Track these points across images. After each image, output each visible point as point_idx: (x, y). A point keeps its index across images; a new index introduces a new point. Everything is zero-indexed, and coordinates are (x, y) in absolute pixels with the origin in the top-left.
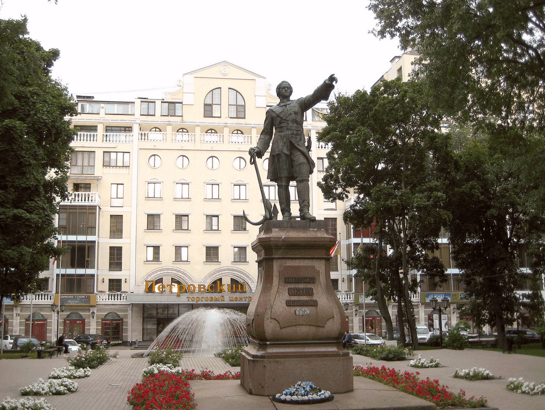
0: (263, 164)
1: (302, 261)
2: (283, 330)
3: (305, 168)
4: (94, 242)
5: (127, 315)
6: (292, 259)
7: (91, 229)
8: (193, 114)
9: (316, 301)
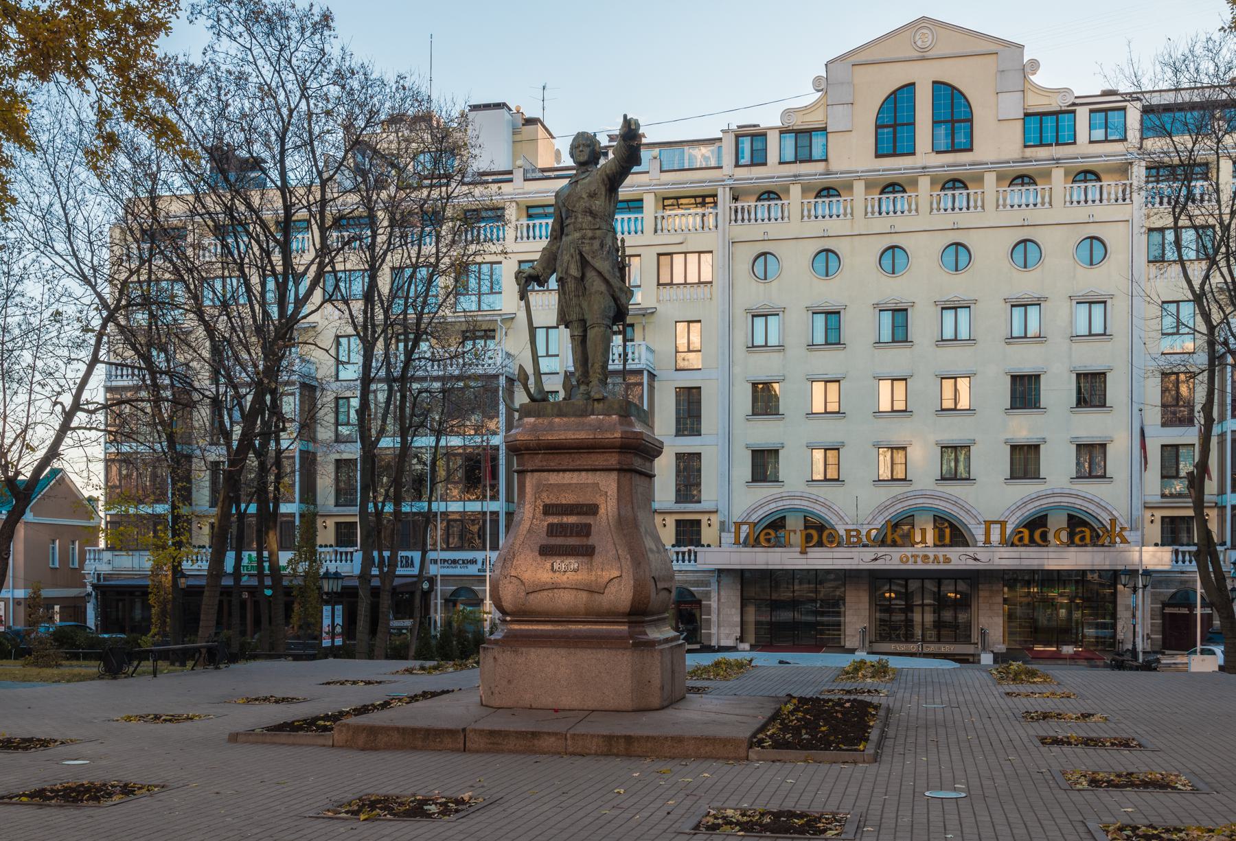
5: (709, 592)
8: (853, 152)
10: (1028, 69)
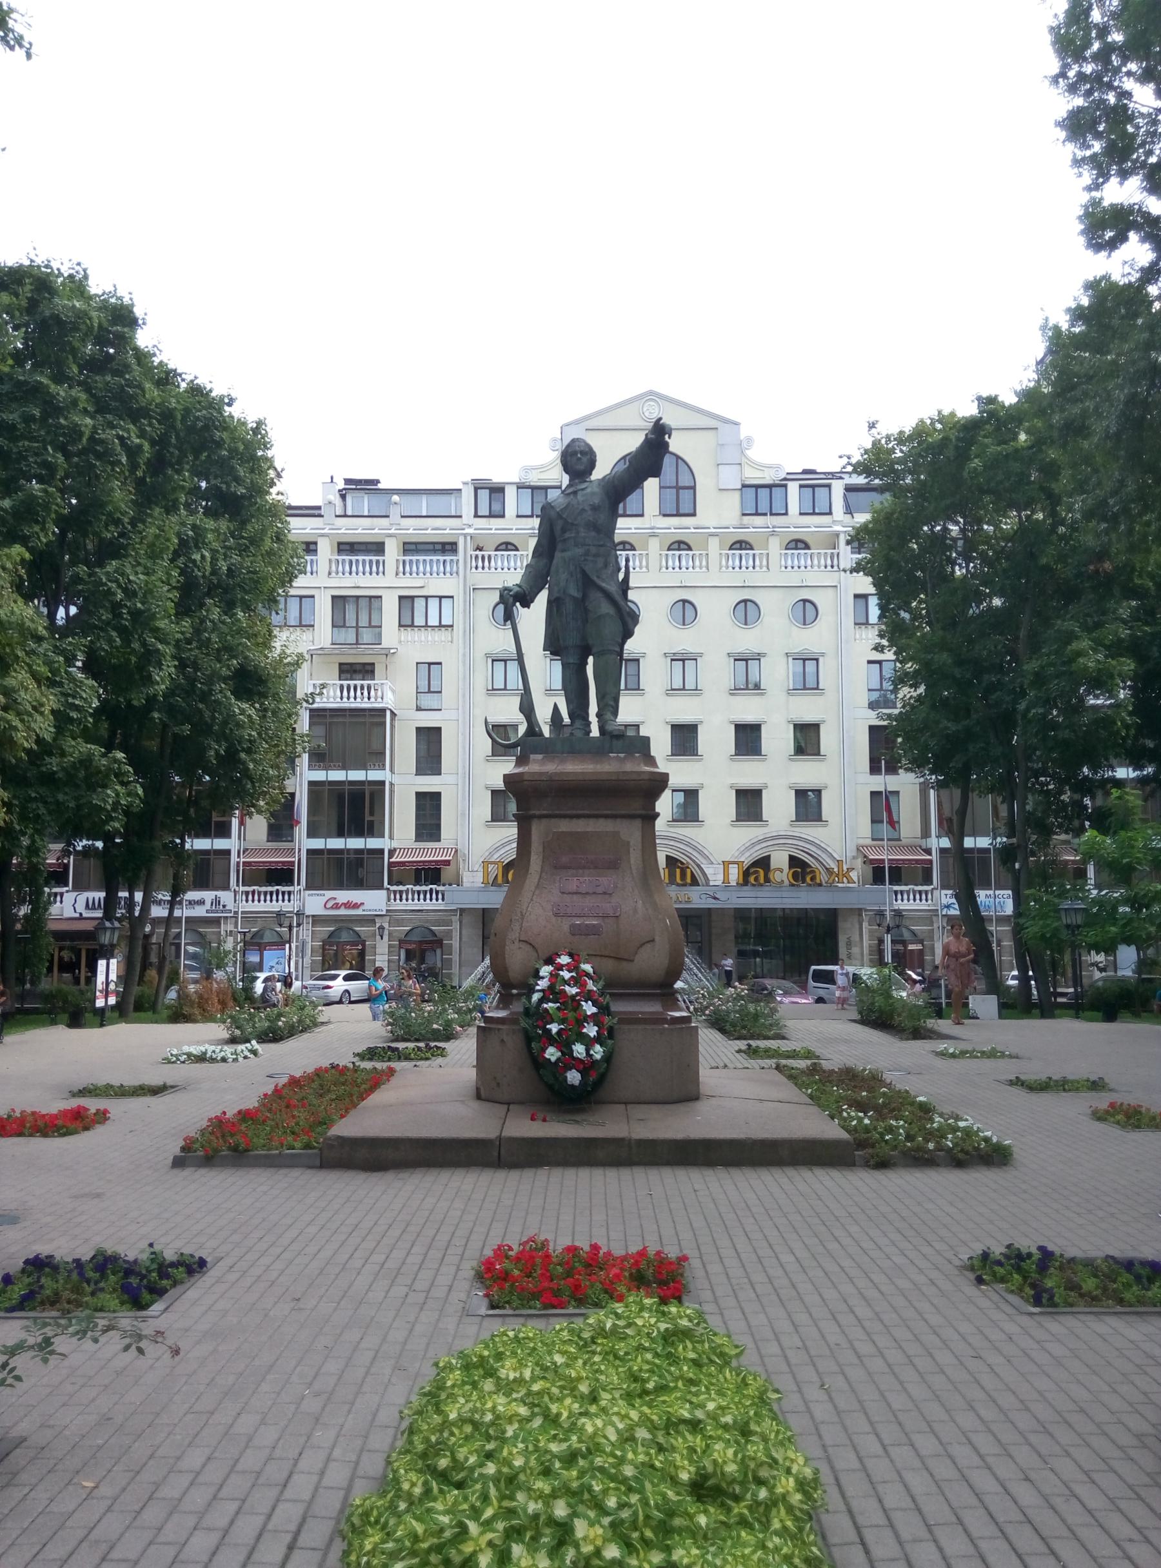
0: (533, 619)
1: (592, 821)
3: (611, 628)
4: (383, 783)
6: (571, 817)
7: (376, 756)
10: (745, 445)
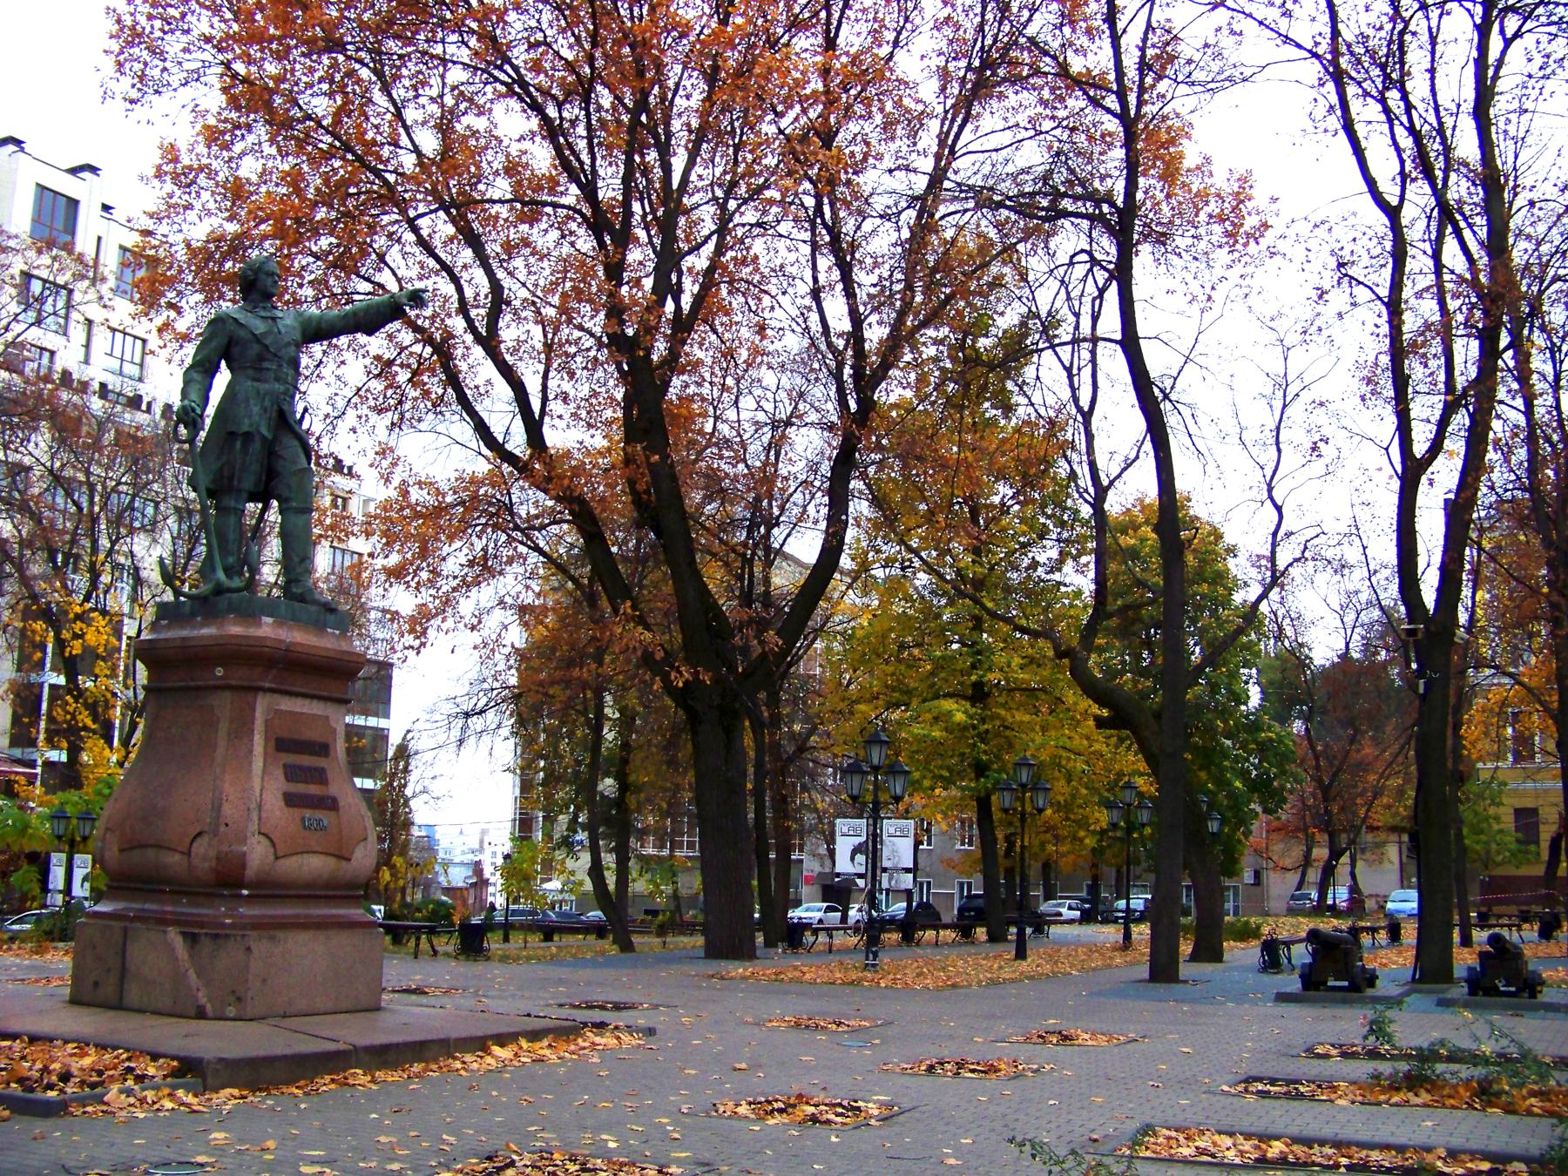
1: (307, 702)
2: (282, 861)
9: (334, 800)
